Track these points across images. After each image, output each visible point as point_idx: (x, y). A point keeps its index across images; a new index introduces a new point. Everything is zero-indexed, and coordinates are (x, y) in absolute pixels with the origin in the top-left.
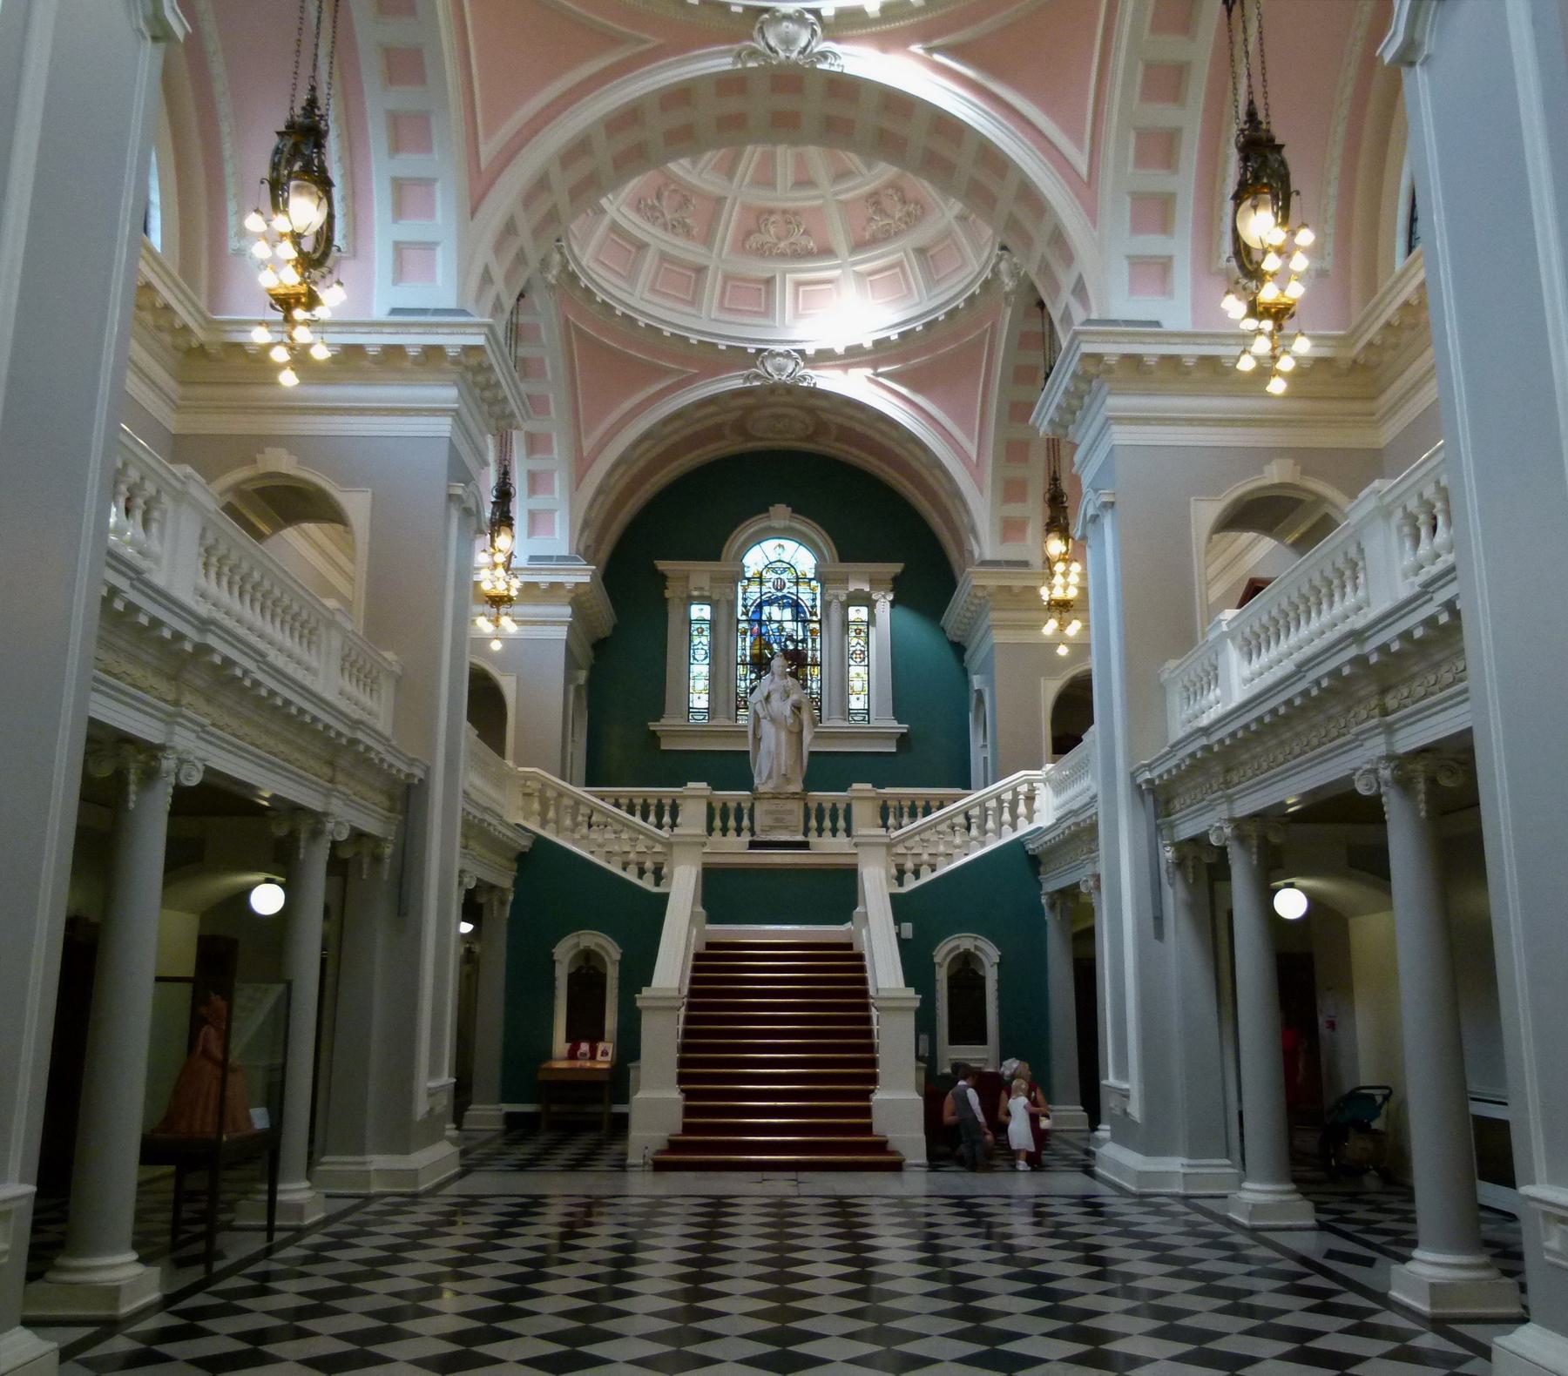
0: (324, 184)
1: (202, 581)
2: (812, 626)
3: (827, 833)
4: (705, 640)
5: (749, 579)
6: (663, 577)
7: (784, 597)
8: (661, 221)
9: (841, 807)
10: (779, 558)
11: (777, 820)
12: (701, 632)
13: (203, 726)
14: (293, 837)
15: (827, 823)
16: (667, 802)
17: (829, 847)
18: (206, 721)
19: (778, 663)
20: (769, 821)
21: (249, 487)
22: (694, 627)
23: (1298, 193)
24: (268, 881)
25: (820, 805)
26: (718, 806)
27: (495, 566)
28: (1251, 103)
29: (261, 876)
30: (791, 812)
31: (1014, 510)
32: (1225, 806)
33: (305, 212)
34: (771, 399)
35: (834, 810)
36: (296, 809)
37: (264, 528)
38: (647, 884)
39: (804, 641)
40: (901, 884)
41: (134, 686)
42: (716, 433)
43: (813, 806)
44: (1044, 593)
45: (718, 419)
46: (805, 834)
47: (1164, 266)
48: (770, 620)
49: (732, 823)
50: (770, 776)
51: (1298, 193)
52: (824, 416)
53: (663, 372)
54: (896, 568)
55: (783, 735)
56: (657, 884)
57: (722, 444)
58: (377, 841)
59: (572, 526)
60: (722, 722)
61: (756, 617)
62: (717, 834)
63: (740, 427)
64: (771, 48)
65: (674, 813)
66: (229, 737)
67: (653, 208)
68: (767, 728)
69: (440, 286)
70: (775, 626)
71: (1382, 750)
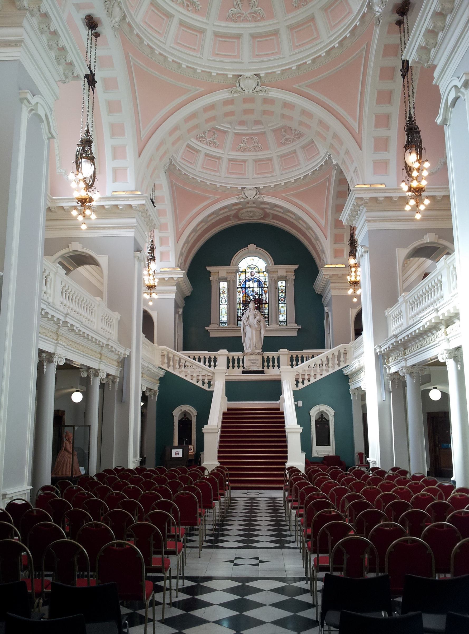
0: (92, 159)
1: (62, 299)
2: (265, 289)
3: (271, 368)
4: (225, 295)
5: (241, 272)
6: (210, 273)
7: (254, 278)
8: (205, 141)
9: (276, 358)
10: (252, 265)
11: (252, 363)
12: (224, 293)
13: (64, 346)
14: (88, 377)
15: (271, 364)
16: (212, 357)
17: (271, 373)
18: (65, 344)
19: (252, 305)
20: (249, 363)
21: (66, 256)
22: (221, 290)
23: (425, 149)
24: (77, 391)
25: (268, 357)
26: (231, 358)
27: (149, 275)
28: (410, 114)
29: (75, 390)
30: (258, 360)
31: (338, 246)
32: (404, 362)
33: (87, 168)
34: (248, 206)
35: (273, 358)
36: (89, 368)
37: (71, 268)
38: (206, 387)
39: (262, 295)
40: (297, 387)
41: (46, 336)
42: (227, 219)
43: (266, 357)
44: (348, 278)
45: (228, 214)
46: (263, 368)
47: (386, 163)
48: (249, 287)
49: (236, 364)
50: (250, 347)
51: (425, 149)
52: (267, 211)
53: (207, 198)
54: (296, 266)
55: (254, 332)
56: (209, 388)
57: (229, 222)
58: (114, 377)
59: (176, 257)
60: (232, 326)
61: (244, 286)
62: (231, 368)
63: (236, 216)
64: (242, 89)
65: (215, 362)
66: (71, 348)
67: (202, 137)
68: (248, 329)
69: (129, 183)
71: (404, 365)
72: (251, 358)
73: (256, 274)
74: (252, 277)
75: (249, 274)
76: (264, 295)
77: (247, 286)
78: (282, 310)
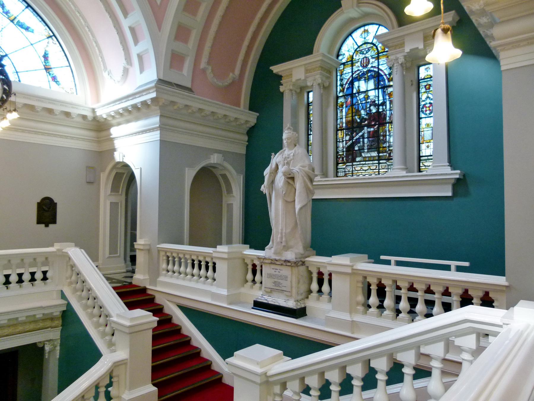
5: (344, 64)
6: (279, 77)
7: (369, 71)
39: (384, 104)
48: (359, 92)
61: (349, 92)
70: (362, 96)
72: (273, 272)
73: (371, 60)
74: (365, 70)
75: (359, 64)
76: (388, 103)
77: (355, 91)
78: (427, 134)
